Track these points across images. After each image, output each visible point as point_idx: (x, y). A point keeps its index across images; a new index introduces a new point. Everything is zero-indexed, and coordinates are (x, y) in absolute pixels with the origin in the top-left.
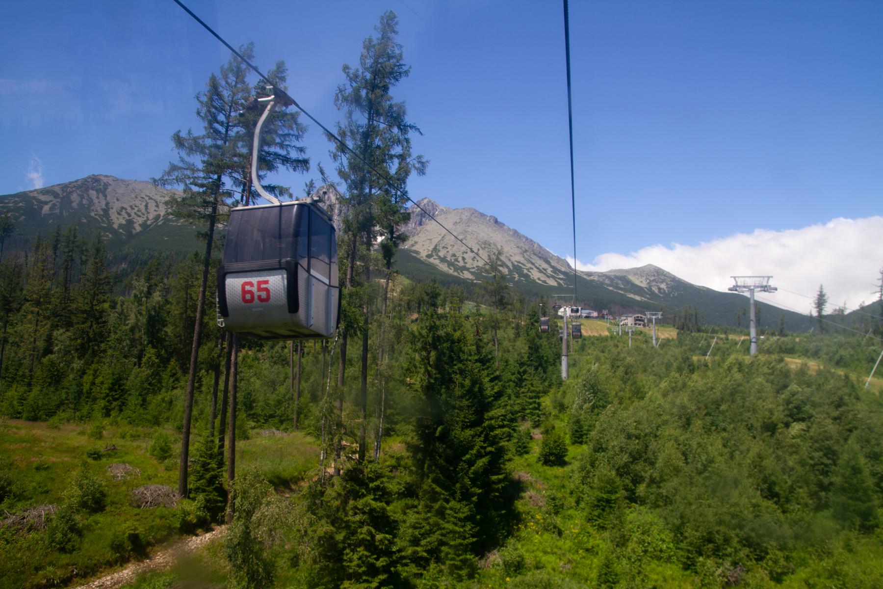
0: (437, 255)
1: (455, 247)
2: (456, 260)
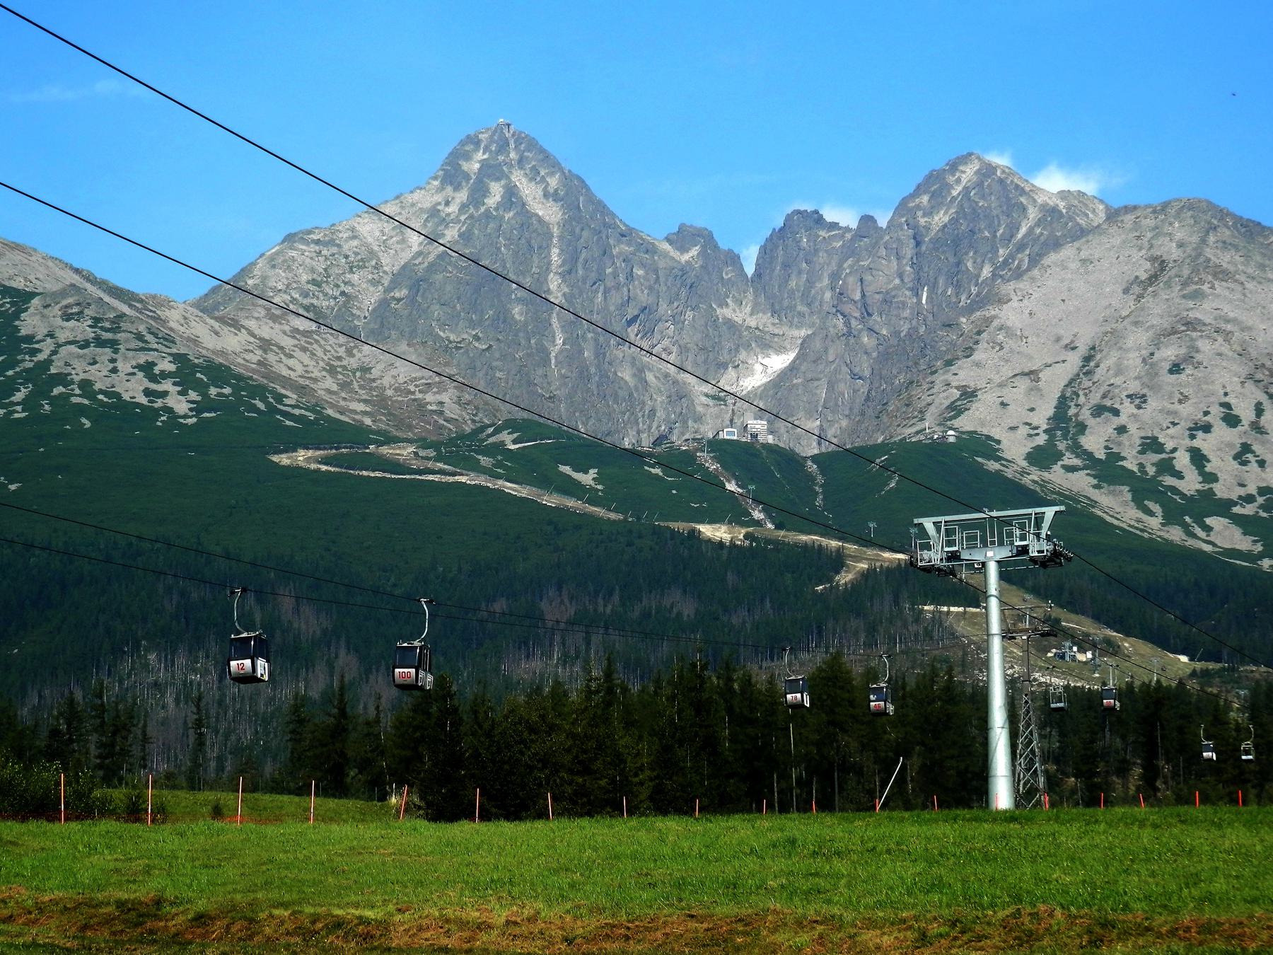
0: (1077, 449)
1: (1153, 404)
2: (1167, 467)
